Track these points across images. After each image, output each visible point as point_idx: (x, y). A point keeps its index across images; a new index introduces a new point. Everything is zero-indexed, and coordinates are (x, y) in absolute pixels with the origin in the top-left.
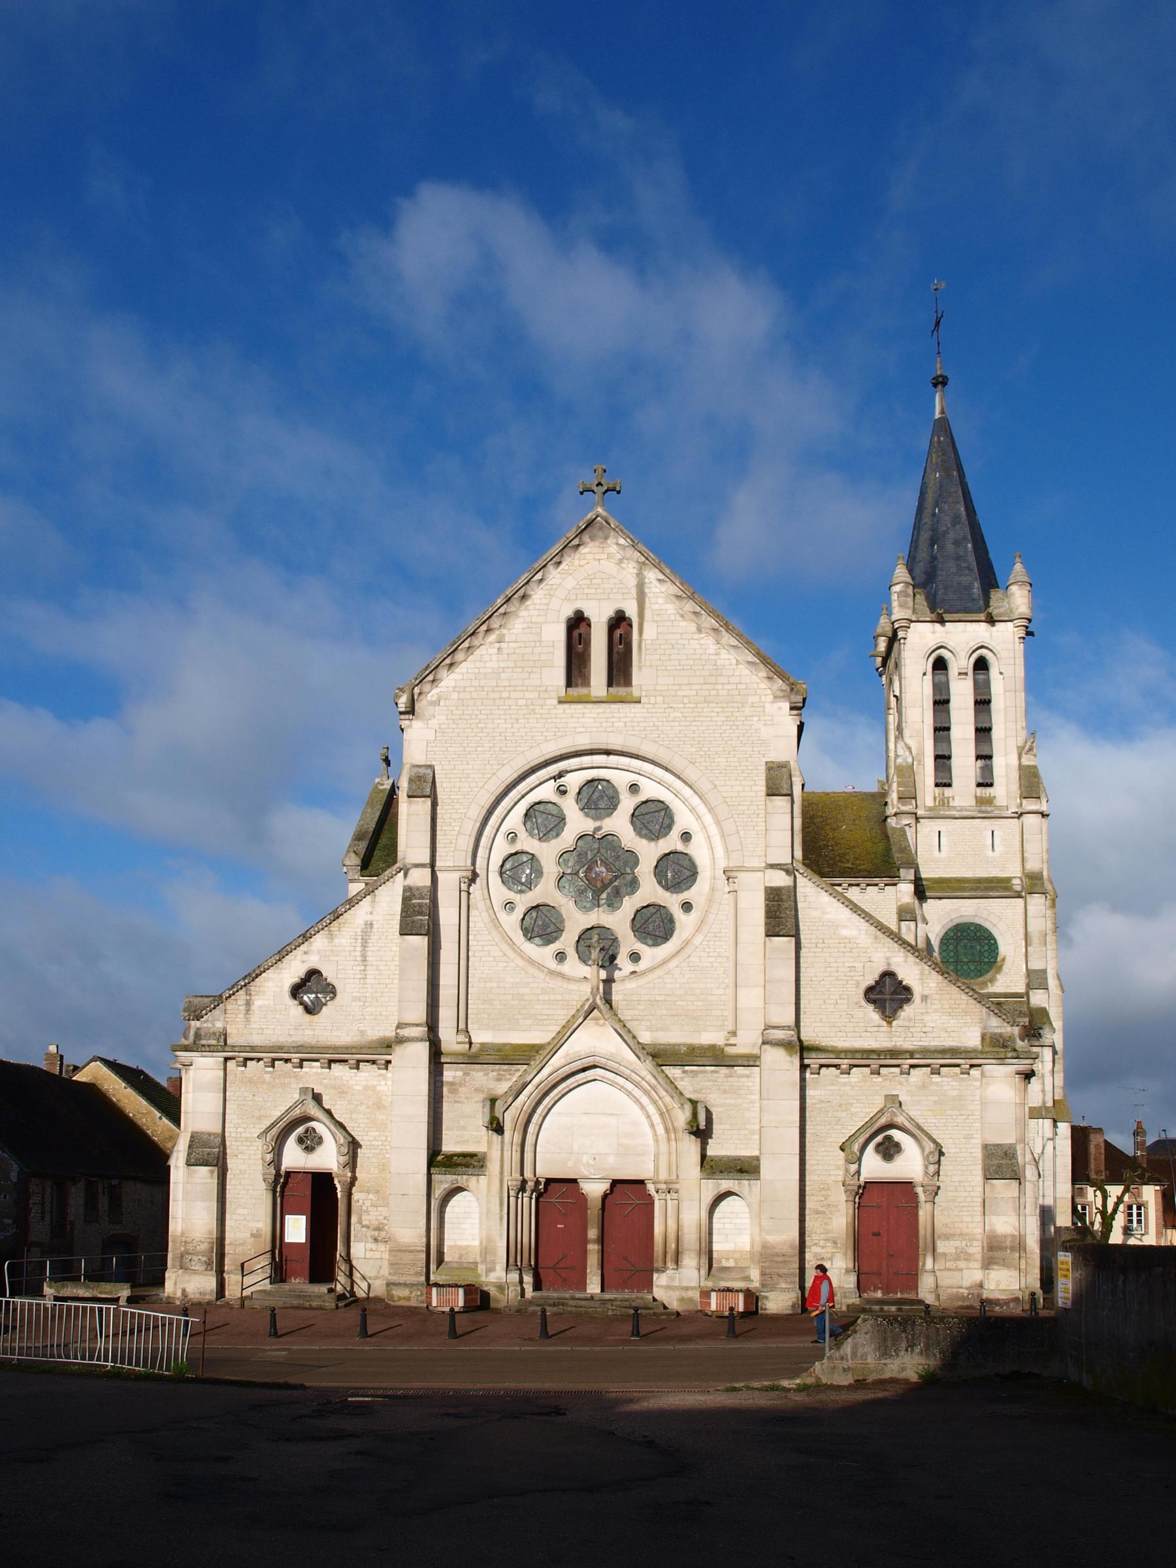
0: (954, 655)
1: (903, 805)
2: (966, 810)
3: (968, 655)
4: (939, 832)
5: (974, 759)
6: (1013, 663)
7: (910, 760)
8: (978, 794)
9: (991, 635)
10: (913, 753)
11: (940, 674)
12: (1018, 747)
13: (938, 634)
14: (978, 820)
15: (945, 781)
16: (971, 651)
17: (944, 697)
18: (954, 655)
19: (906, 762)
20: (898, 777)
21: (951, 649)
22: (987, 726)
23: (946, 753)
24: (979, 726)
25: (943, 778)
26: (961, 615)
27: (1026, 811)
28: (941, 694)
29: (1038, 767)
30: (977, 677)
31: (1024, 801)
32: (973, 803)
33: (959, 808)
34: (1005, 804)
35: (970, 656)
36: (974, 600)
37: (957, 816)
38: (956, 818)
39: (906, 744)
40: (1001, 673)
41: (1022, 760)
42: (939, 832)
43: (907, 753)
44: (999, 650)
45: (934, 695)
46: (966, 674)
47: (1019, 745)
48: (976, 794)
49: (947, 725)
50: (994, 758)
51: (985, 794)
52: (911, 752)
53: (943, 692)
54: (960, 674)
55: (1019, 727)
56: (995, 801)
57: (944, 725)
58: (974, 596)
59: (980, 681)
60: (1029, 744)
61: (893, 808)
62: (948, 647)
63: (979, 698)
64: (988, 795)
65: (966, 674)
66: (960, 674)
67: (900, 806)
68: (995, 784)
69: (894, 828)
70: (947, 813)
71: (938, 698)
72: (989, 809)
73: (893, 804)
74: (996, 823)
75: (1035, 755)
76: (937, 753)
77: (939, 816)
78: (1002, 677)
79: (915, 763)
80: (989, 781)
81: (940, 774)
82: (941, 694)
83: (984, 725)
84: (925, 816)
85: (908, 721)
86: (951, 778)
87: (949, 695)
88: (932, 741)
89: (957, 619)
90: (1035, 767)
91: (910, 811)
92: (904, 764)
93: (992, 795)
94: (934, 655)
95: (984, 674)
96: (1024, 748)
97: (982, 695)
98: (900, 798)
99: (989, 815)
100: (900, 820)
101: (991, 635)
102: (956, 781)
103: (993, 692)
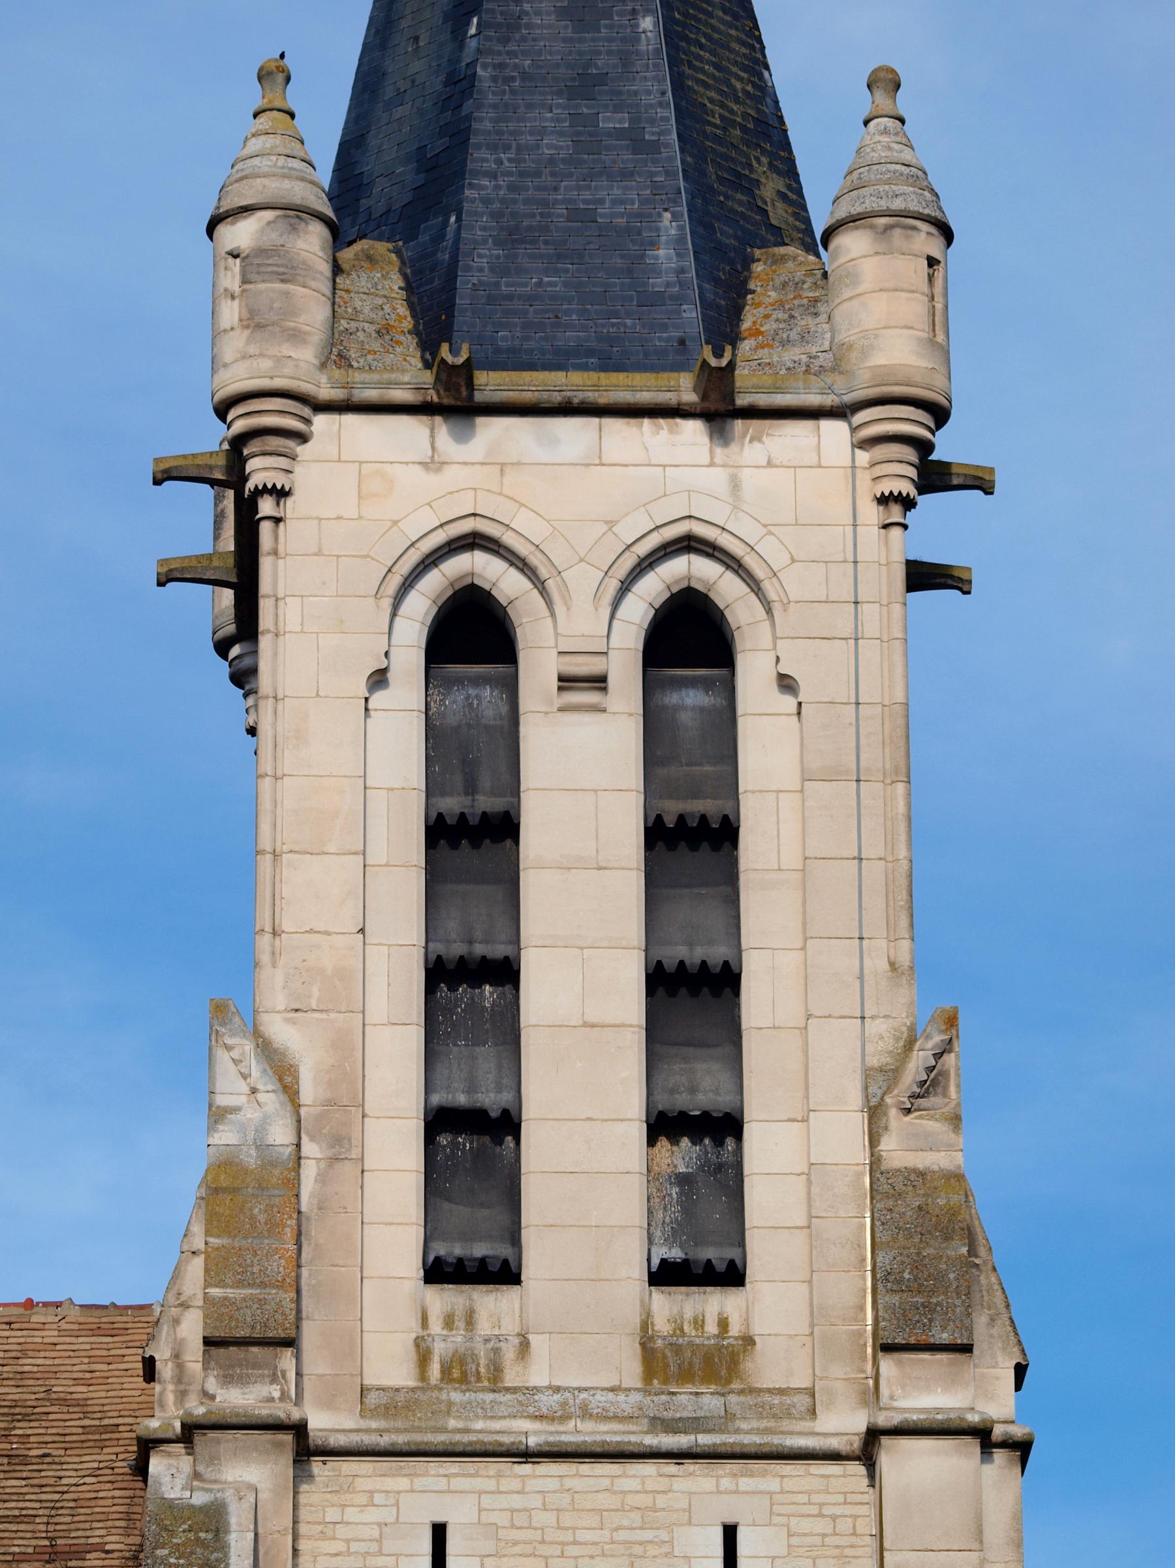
0: (540, 585)
1: (227, 1380)
2: (586, 1413)
3: (613, 585)
4: (439, 1532)
5: (638, 1131)
6: (848, 631)
7: (280, 1135)
8: (662, 1325)
9: (735, 485)
10: (308, 1092)
11: (477, 681)
12: (868, 1074)
13: (452, 476)
14: (648, 1469)
15: (480, 1250)
16: (628, 562)
17: (487, 803)
18: (540, 585)
19: (262, 1147)
20: (208, 1233)
21: (522, 548)
22: (716, 954)
23: (491, 1100)
24: (674, 953)
25: (466, 1237)
26: (591, 377)
27: (895, 1419)
28: (471, 788)
29: (973, 1181)
30: (672, 698)
31: (888, 1365)
32: (631, 1371)
33: (547, 1401)
34: (801, 1380)
35: (625, 587)
36: (651, 300)
37: (532, 1442)
38: (526, 1455)
39: (267, 1050)
40: (786, 684)
41: (888, 1144)
42: (439, 1532)
43: (271, 1100)
44: (778, 559)
45: (432, 788)
46: (599, 682)
47: (874, 1061)
48: (646, 1325)
49: (498, 951)
50: (750, 1131)
51: (699, 1323)
52: (290, 1091)
53: (485, 781)
54: (567, 682)
55: (877, 964)
56: (748, 1365)
57: (480, 950)
58: (657, 284)
59: (685, 718)
60: (920, 1059)
61: (182, 1395)
62: (509, 539)
63: (672, 809)
64: (712, 1328)
65: (599, 682)
66: (567, 682)
67: (212, 1385)
68: (753, 1272)
69: (170, 1505)
70: (479, 1425)
71: (451, 805)
72: (711, 1403)
73: (180, 1376)
74: (745, 1483)
75: (955, 1120)
76: (436, 1099)
77: (437, 1439)
78: (789, 702)
79: (309, 1148)
80: (716, 1254)
81: (456, 1213)
82: (471, 788)
83: (694, 955)
84: (369, 1440)
85: (287, 925)
86: (514, 1238)
87: (514, 789)
88: (413, 1038)
89: (557, 398)
90: (956, 1178)
91: (264, 1412)
92: (250, 1158)
93: (735, 1330)
94: (435, 584)
95: (707, 685)
96: (892, 1074)
97: (695, 795)
98: (208, 1342)
99: (705, 1440)
100: (214, 1460)
101: (735, 485)
102: (533, 1265)
103: (745, 782)
